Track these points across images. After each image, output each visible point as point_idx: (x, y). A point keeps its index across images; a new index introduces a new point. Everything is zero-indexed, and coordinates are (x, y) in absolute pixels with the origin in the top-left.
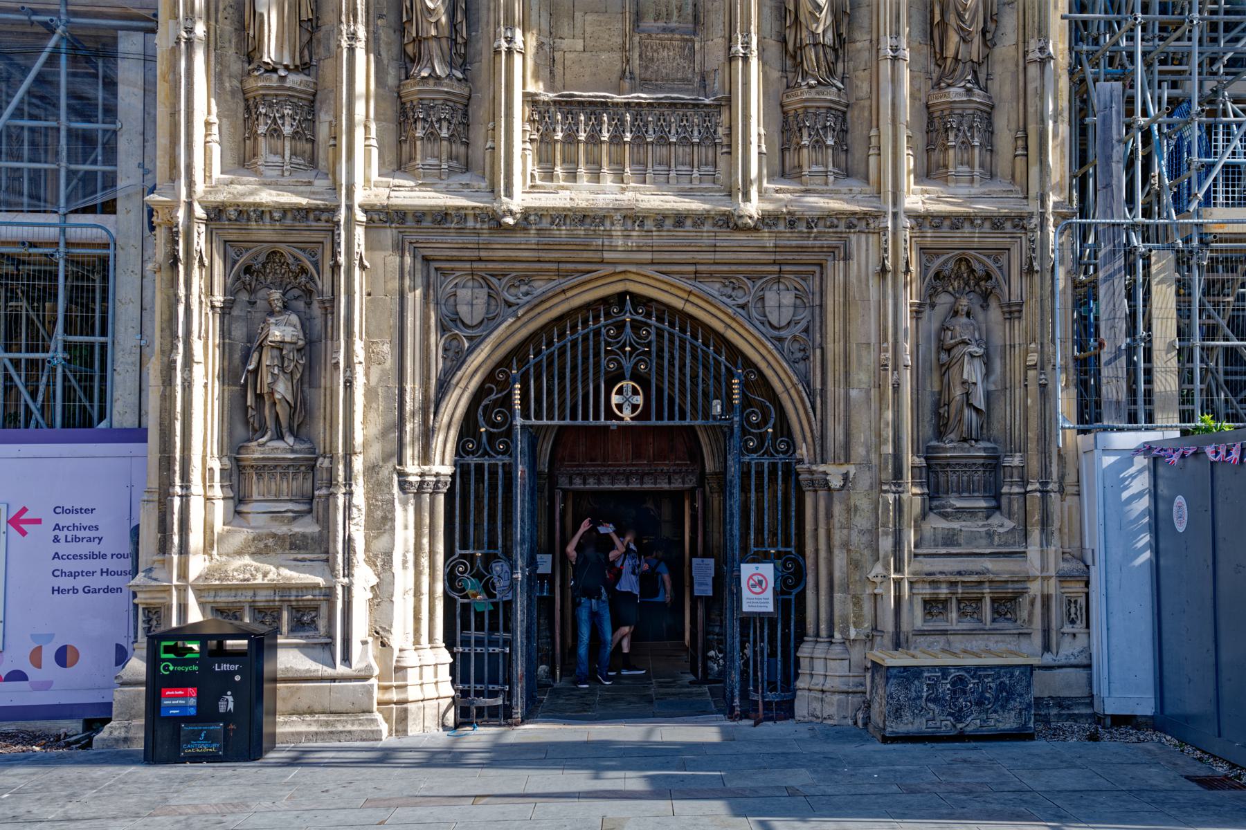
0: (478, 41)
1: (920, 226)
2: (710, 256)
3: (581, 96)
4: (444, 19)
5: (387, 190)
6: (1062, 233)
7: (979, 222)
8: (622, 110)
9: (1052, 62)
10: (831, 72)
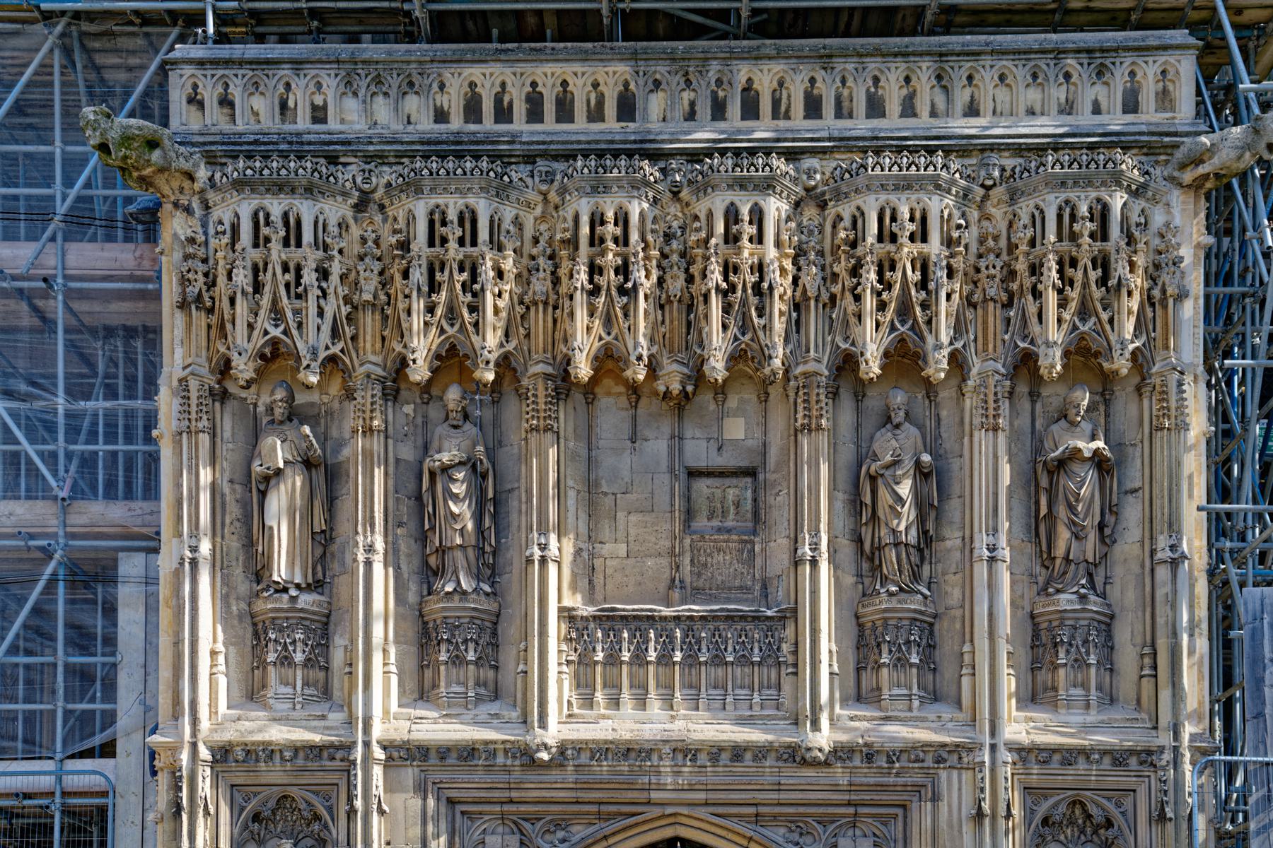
0: (508, 549)
1: (1024, 761)
2: (774, 796)
3: (624, 610)
4: (470, 526)
5: (408, 723)
6: (1201, 773)
7: (1097, 756)
8: (672, 625)
9: (1186, 562)
10: (916, 577)
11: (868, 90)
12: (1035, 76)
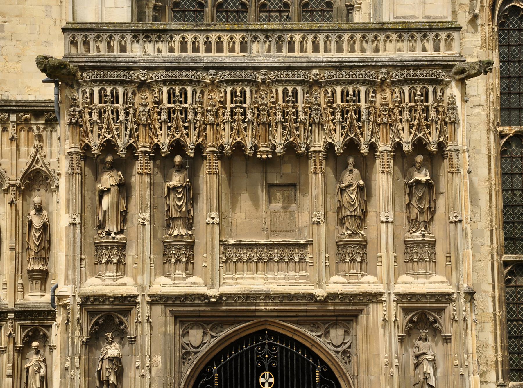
3: (245, 242)
4: (184, 209)
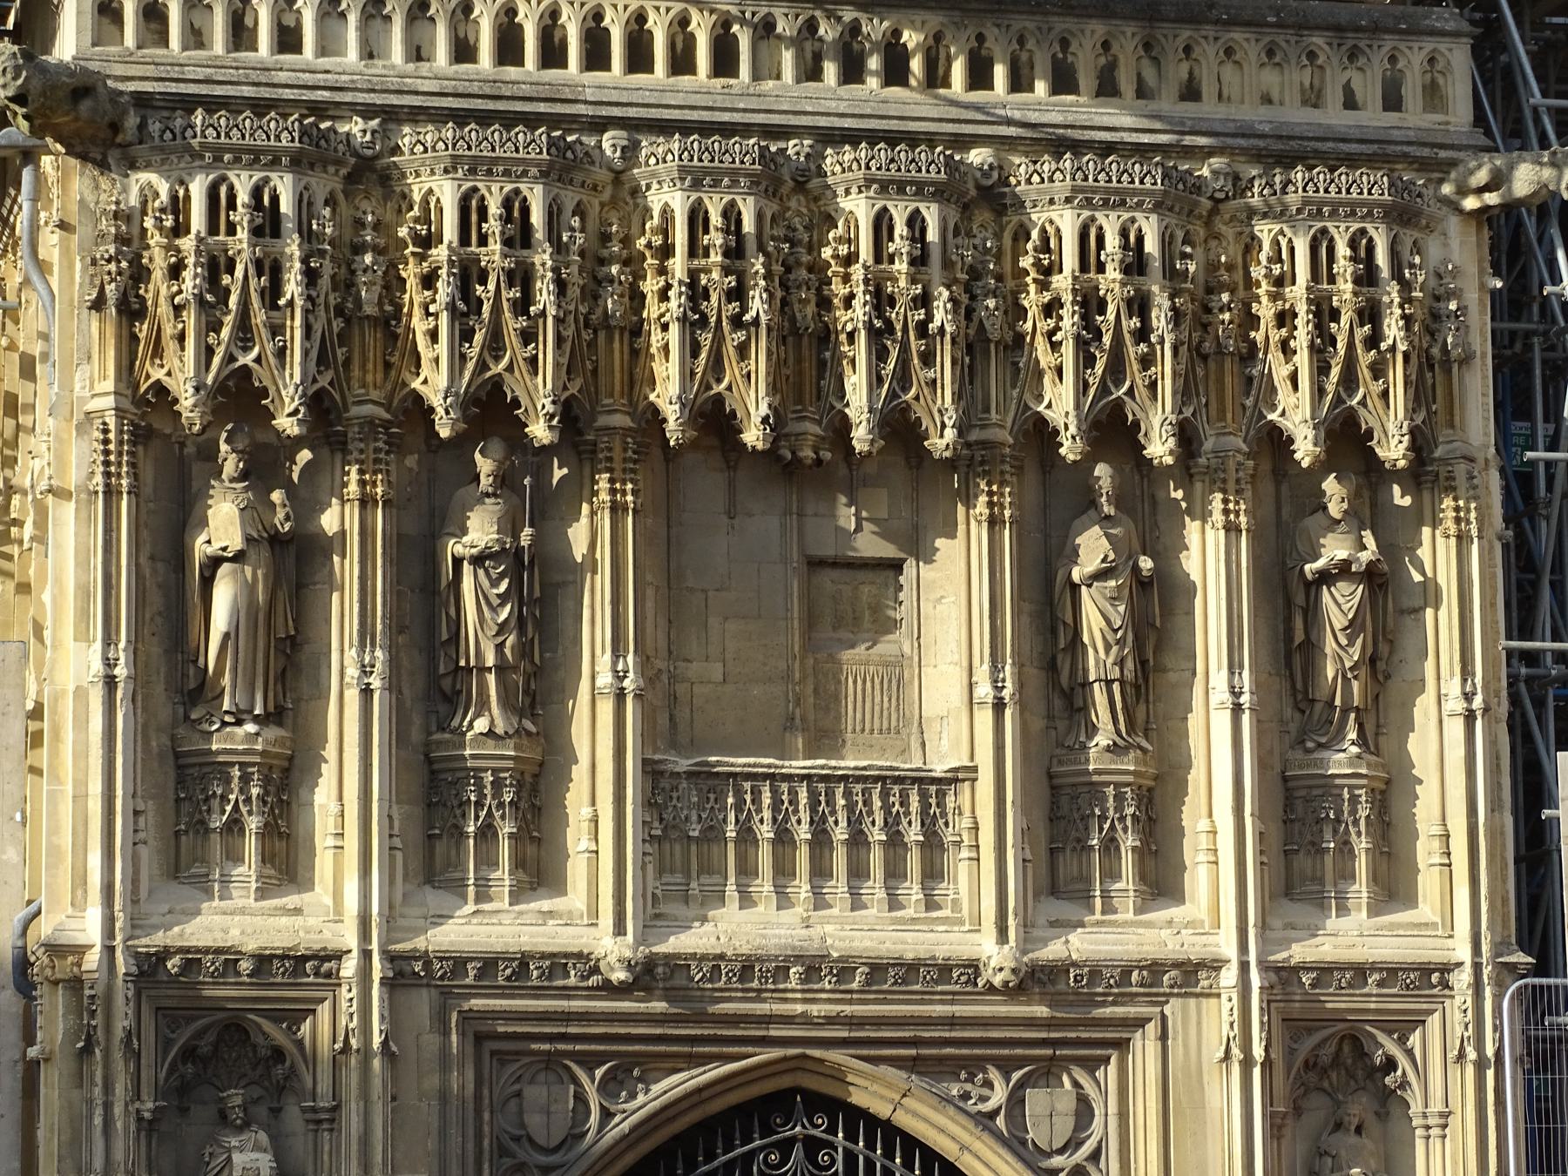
3: (732, 765)
11: (1054, 56)
12: (1270, 53)
